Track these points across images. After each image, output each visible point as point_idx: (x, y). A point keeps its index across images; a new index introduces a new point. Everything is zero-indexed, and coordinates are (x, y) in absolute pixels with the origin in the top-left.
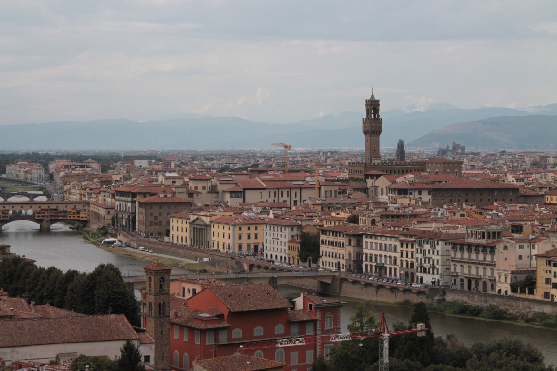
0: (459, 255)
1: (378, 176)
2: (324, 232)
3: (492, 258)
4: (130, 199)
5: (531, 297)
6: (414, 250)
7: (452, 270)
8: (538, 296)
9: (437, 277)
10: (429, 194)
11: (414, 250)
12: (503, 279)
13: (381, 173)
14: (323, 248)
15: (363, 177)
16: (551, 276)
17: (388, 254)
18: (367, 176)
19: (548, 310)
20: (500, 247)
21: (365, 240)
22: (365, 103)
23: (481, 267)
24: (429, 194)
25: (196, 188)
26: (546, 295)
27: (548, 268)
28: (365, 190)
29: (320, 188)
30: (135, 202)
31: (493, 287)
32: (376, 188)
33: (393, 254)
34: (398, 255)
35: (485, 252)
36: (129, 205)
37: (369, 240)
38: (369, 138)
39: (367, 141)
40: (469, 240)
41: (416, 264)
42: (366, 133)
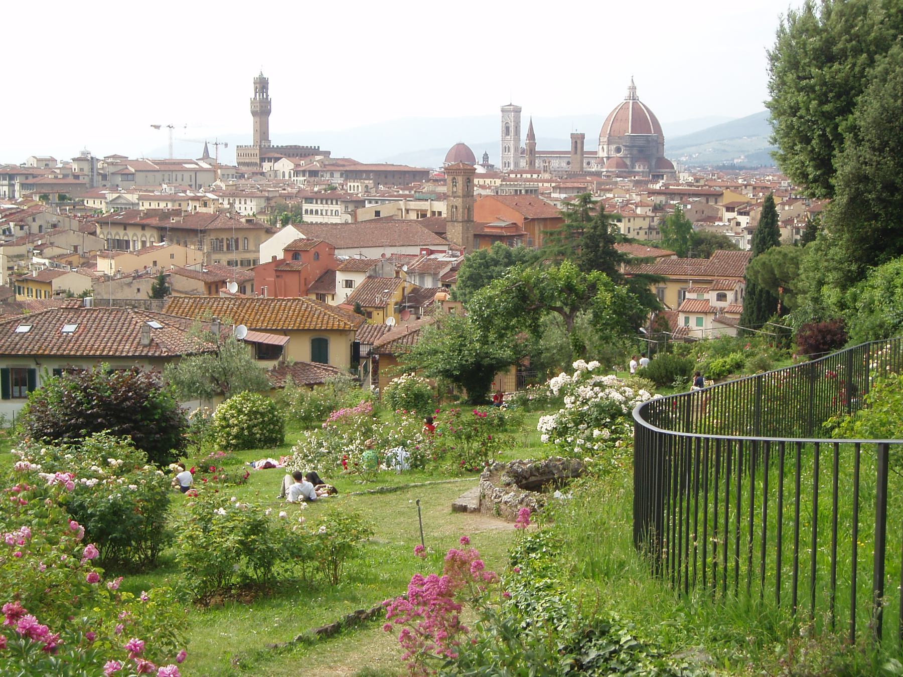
1: (277, 160)
2: (309, 200)
4: (6, 182)
10: (341, 177)
13: (279, 156)
15: (258, 161)
18: (262, 160)
22: (253, 81)
24: (341, 177)
25: (82, 170)
28: (262, 174)
30: (13, 185)
36: (6, 189)
38: (258, 119)
39: (255, 122)
42: (254, 113)
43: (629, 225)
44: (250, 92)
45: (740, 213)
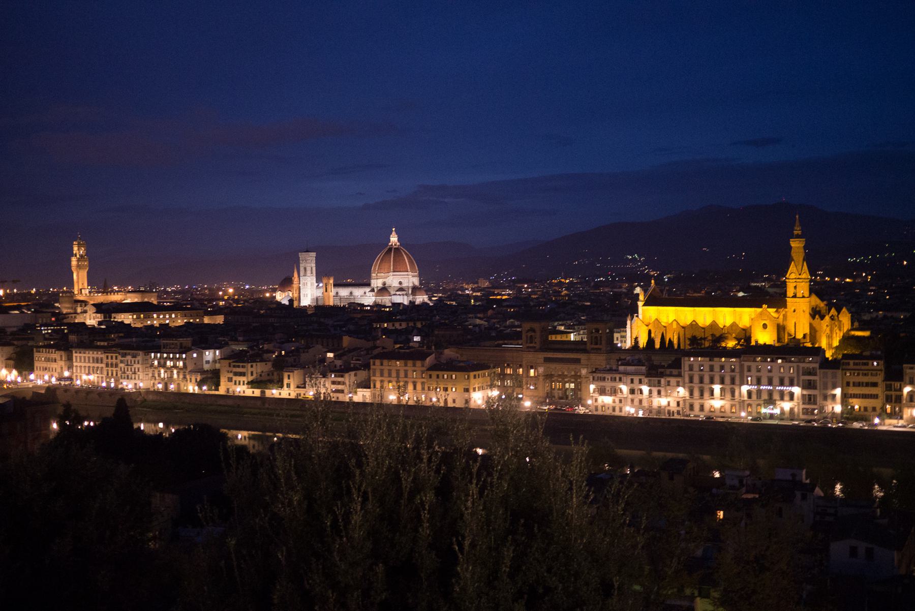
6: (118, 361)
11: (118, 361)
12: (193, 380)
14: (37, 364)
17: (96, 365)
19: (230, 402)
21: (74, 355)
27: (230, 369)
34: (103, 365)
37: (78, 355)
41: (119, 373)
43: (250, 369)
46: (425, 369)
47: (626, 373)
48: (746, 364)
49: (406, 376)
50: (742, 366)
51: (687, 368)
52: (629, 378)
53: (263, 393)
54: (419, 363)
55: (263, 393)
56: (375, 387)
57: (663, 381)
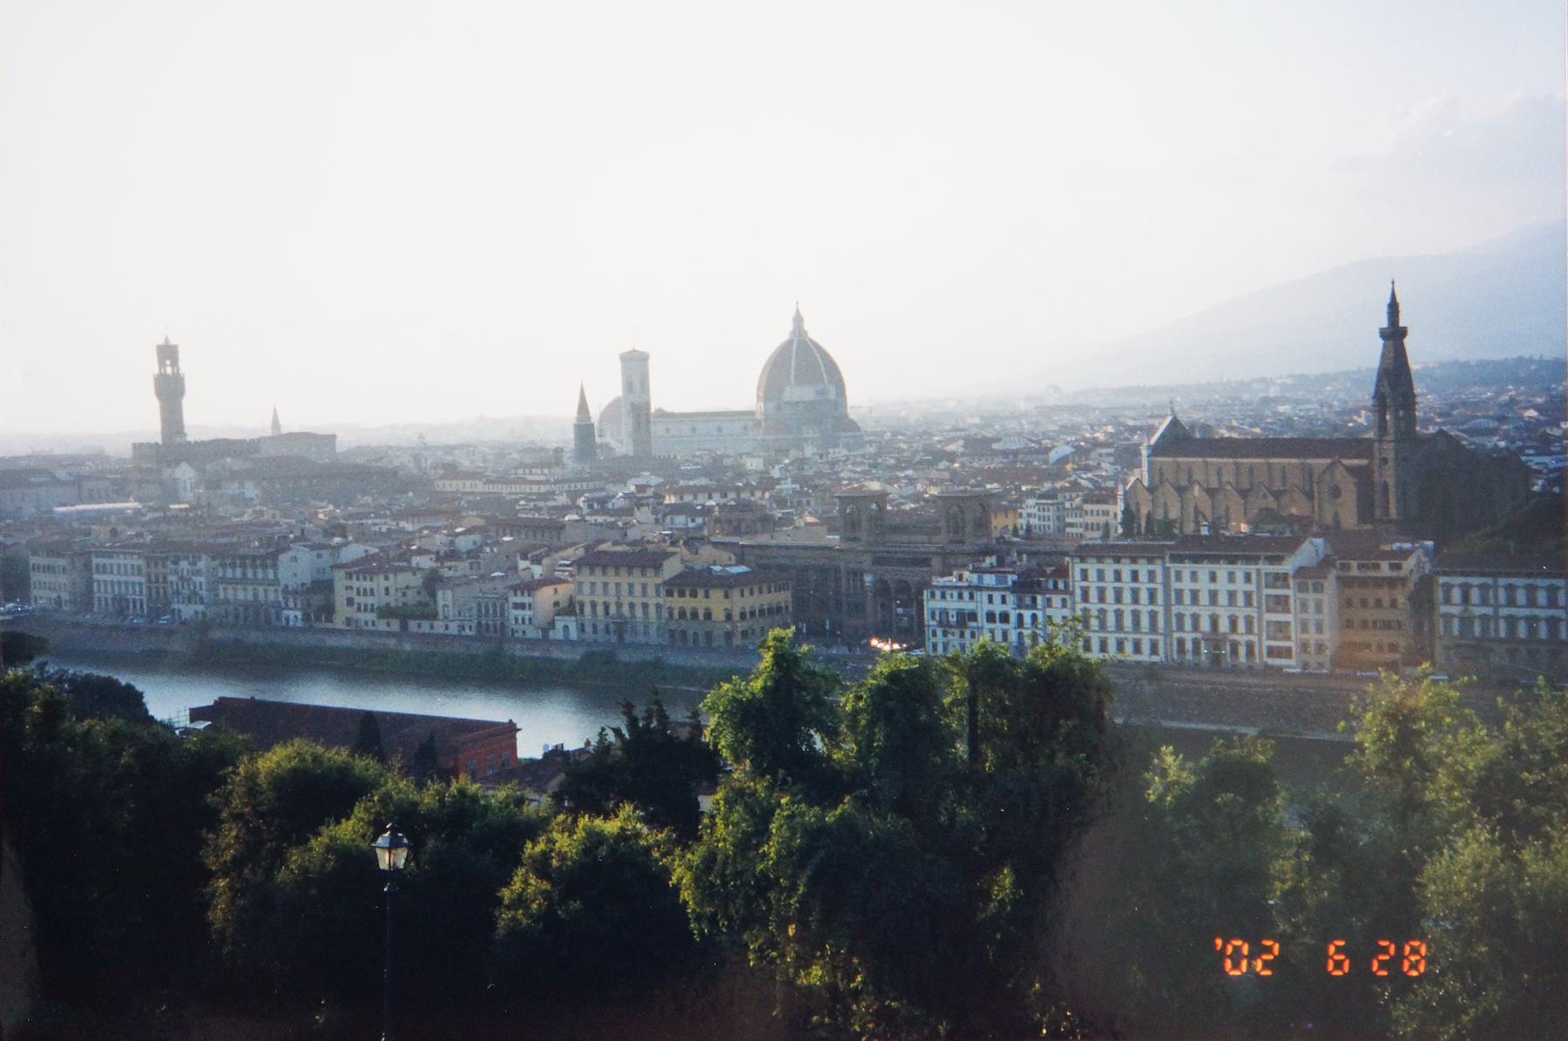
0: (229, 573)
1: (178, 464)
2: (35, 553)
3: (276, 574)
5: (329, 625)
7: (222, 596)
8: (339, 622)
9: (201, 608)
14: (35, 577)
16: (353, 594)
19: (347, 642)
20: (284, 558)
23: (261, 589)
26: (348, 621)
27: (349, 583)
29: (80, 486)
31: (278, 618)
32: (175, 480)
33: (137, 579)
34: (143, 580)
35: (265, 567)
37: (101, 561)
40: (242, 551)
41: (170, 590)
44: (151, 366)
45: (533, 562)
46: (659, 581)
47: (980, 588)
48: (1174, 567)
49: (631, 593)
50: (1166, 571)
51: (1078, 576)
52: (985, 595)
53: (404, 627)
54: (650, 572)
55: (404, 627)
56: (582, 612)
57: (1039, 598)
